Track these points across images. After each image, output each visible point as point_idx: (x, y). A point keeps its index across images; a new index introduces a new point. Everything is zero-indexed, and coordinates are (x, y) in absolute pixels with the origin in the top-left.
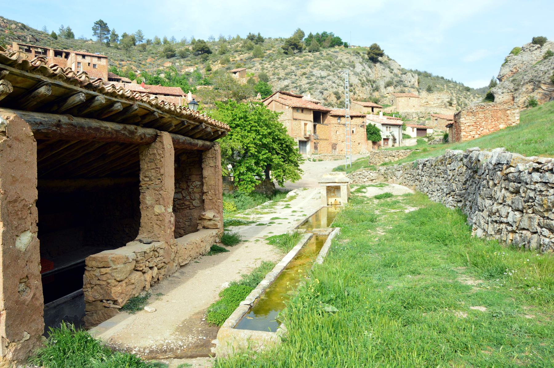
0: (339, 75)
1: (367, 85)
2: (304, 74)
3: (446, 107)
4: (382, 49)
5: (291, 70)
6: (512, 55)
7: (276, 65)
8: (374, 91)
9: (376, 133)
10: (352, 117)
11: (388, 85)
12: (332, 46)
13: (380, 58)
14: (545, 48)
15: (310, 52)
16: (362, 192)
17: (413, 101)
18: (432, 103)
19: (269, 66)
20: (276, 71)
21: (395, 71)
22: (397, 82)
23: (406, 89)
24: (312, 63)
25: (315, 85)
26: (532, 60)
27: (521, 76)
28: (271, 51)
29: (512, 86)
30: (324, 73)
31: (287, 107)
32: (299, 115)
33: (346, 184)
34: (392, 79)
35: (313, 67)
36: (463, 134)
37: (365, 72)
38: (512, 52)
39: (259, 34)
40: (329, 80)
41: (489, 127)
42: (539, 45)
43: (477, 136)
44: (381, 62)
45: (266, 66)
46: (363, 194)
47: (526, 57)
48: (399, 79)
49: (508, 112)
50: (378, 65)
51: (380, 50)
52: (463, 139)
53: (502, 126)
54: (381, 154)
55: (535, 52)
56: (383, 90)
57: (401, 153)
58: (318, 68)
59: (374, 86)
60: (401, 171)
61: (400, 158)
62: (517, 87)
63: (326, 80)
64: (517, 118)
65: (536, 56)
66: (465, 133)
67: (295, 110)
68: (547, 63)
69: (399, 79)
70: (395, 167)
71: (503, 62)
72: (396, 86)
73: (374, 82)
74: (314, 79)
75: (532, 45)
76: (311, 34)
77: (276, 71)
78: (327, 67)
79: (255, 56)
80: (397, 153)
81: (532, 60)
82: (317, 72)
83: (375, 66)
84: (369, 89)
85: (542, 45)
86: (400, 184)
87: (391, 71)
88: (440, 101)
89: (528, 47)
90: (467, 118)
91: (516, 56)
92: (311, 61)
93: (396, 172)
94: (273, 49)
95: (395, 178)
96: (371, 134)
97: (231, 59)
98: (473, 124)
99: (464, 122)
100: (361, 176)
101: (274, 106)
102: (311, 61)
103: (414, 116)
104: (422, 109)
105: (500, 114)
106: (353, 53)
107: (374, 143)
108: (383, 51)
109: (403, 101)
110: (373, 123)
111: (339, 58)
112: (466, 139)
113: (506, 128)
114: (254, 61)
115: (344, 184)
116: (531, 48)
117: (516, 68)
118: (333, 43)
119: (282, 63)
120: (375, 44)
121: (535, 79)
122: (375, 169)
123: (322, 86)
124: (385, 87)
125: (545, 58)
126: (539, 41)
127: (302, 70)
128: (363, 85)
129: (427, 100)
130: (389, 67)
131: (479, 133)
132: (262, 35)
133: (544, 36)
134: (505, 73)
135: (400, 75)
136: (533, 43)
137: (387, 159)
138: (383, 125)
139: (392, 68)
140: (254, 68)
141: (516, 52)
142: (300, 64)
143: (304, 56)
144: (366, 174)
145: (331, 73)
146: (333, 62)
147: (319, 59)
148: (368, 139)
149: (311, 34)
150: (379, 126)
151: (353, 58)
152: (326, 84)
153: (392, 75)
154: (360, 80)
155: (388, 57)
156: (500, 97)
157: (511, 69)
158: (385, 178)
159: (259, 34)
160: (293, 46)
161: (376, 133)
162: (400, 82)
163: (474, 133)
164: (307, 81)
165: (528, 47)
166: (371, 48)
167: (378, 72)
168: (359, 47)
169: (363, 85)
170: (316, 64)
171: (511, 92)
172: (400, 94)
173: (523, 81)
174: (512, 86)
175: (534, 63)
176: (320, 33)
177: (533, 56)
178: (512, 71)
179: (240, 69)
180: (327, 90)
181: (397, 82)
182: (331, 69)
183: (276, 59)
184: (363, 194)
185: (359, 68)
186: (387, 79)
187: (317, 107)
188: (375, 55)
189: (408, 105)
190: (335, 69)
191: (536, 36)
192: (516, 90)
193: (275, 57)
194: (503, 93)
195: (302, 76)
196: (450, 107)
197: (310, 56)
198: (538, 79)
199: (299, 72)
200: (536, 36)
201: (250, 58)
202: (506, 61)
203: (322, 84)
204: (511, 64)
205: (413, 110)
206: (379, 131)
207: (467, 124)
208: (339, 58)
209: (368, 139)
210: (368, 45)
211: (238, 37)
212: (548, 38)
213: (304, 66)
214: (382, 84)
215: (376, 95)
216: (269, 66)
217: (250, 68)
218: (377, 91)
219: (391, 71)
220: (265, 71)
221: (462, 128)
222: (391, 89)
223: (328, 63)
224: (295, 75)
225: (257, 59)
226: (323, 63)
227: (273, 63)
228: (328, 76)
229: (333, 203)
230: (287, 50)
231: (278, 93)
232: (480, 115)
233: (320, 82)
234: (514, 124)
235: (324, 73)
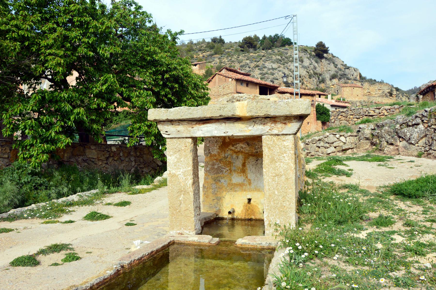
0: (289, 68)
1: (314, 77)
2: (258, 66)
3: (387, 96)
4: (327, 46)
5: (246, 63)
7: (233, 59)
8: (320, 82)
9: (325, 114)
10: (302, 95)
11: (333, 77)
12: (283, 45)
13: (325, 55)
15: (263, 50)
16: (340, 173)
17: (357, 91)
18: (374, 93)
19: (227, 60)
20: (233, 64)
21: (339, 66)
22: (341, 76)
23: (350, 81)
24: (265, 58)
25: (267, 75)
28: (230, 50)
30: (275, 66)
31: (230, 80)
32: (242, 88)
33: (293, 126)
34: (337, 72)
35: (265, 61)
37: (312, 66)
39: (220, 37)
40: (280, 71)
44: (326, 58)
45: (223, 60)
46: (346, 180)
48: (343, 72)
50: (323, 60)
51: (325, 47)
54: (350, 112)
56: (328, 82)
57: (384, 111)
58: (270, 62)
59: (321, 78)
60: (421, 126)
63: (276, 71)
67: (239, 84)
69: (343, 72)
70: (401, 121)
72: (340, 78)
73: (320, 75)
74: (266, 70)
76: (265, 36)
77: (233, 64)
78: (278, 61)
79: (216, 53)
80: (377, 111)
82: (268, 65)
83: (321, 61)
84: (315, 80)
86: (419, 156)
87: (336, 66)
88: (381, 92)
92: (263, 56)
93: (405, 130)
94: (232, 48)
95: (402, 144)
96: (320, 114)
97: (195, 56)
100: (322, 144)
101: (217, 80)
102: (263, 56)
103: (358, 104)
104: (366, 98)
106: (301, 50)
107: (324, 123)
108: (328, 48)
109: (348, 90)
110: (321, 104)
111: (289, 54)
114: (214, 57)
115: (278, 128)
118: (284, 43)
119: (238, 57)
120: (321, 42)
122: (349, 130)
123: (273, 76)
124: (331, 80)
127: (255, 63)
128: (310, 77)
129: (369, 91)
130: (334, 63)
132: (222, 38)
135: (343, 70)
138: (332, 106)
139: (336, 63)
140: (213, 63)
142: (254, 58)
143: (258, 52)
144: (332, 138)
145: (283, 66)
146: (283, 57)
147: (271, 54)
148: (318, 119)
149: (265, 36)
150: (328, 107)
151: (302, 54)
152: (276, 74)
153: (336, 69)
154: (308, 73)
155: (332, 55)
158: (373, 144)
159: (220, 37)
160: (249, 44)
161: (325, 114)
162: (344, 76)
164: (259, 72)
166: (317, 46)
167: (324, 67)
168: (307, 46)
169: (310, 77)
170: (269, 59)
172: (344, 85)
176: (273, 35)
179: (200, 62)
180: (277, 79)
181: (341, 76)
182: (281, 63)
183: (233, 55)
184: (346, 180)
185: (307, 62)
186: (332, 73)
187: (263, 82)
188: (320, 51)
189: (352, 94)
190: (285, 62)
193: (232, 53)
195: (255, 68)
196: (391, 97)
197: (263, 53)
199: (252, 65)
201: (211, 55)
203: (273, 74)
205: (357, 99)
206: (328, 111)
208: (289, 54)
209: (318, 119)
210: (313, 44)
211: (204, 40)
213: (258, 60)
214: (327, 76)
215: (322, 86)
216: (227, 60)
217: (210, 62)
218: (323, 83)
219: (336, 66)
220: (223, 64)
222: (335, 81)
223: (280, 58)
224: (249, 67)
225: (217, 55)
226: (274, 58)
227: (230, 58)
228: (279, 68)
229: (239, 213)
230: (243, 48)
231: (224, 70)
233: (271, 73)
235: (275, 66)
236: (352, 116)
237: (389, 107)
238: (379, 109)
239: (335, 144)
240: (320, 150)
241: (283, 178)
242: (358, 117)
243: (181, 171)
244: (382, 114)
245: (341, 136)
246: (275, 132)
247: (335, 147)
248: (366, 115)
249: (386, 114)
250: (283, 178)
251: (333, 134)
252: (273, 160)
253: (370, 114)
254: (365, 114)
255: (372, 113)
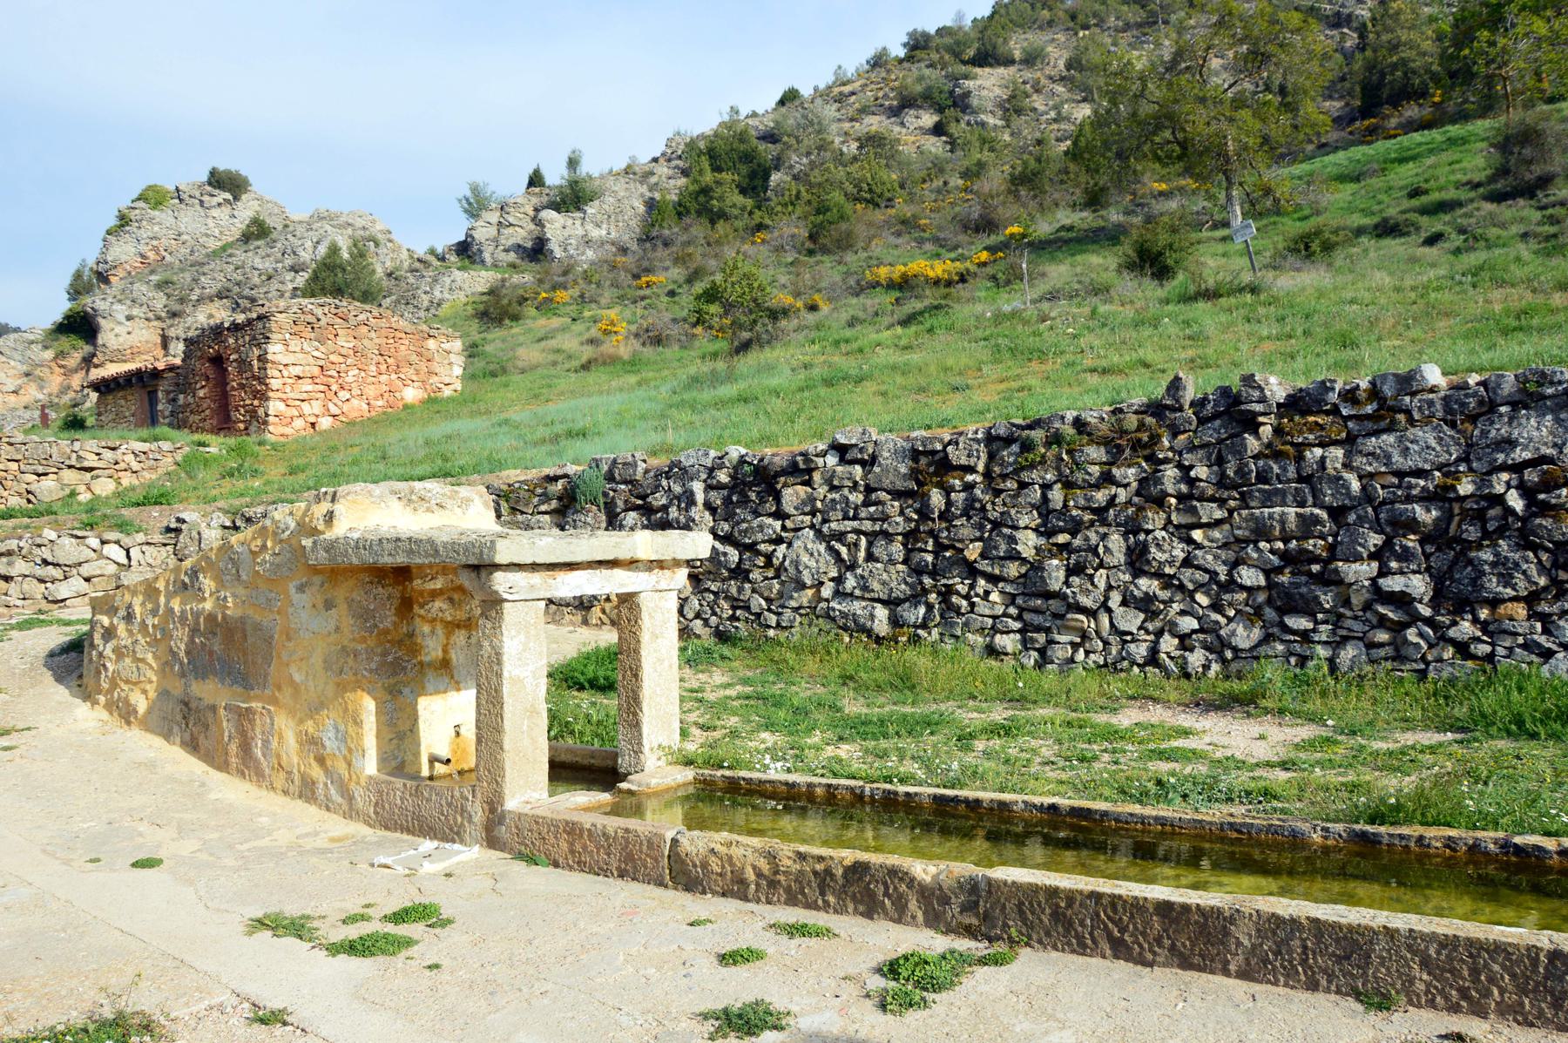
6: (141, 204)
14: (246, 210)
26: (207, 235)
27: (188, 276)
29: (160, 302)
36: (275, 406)
38: (141, 198)
41: (371, 391)
42: (228, 196)
43: (325, 423)
47: (189, 221)
49: (431, 343)
52: (275, 431)
53: (411, 394)
55: (215, 212)
57: (130, 458)
61: (127, 480)
62: (176, 307)
64: (458, 371)
65: (218, 225)
66: (281, 406)
68: (269, 251)
71: (112, 221)
75: (209, 188)
80: (108, 455)
81: (207, 235)
85: (236, 198)
89: (197, 194)
90: (295, 344)
91: (157, 213)
98: (316, 371)
99: (277, 358)
100: (20, 567)
105: (404, 349)
112: (288, 430)
113: (422, 402)
116: (206, 198)
117: (156, 249)
121: (236, 289)
125: (246, 238)
126: (227, 183)
131: (334, 410)
133: (243, 173)
134: (124, 258)
136: (210, 184)
137: (48, 483)
141: (153, 197)
156: (118, 329)
157: (143, 248)
163: (316, 407)
165: (197, 194)
171: (159, 318)
173: (197, 291)
174: (160, 302)
175: (213, 244)
177: (210, 222)
178: (142, 256)
191: (222, 166)
192: (174, 315)
194: (129, 318)
198: (246, 292)
200: (222, 167)
202: (124, 220)
204: (143, 234)
207: (297, 371)
212: (251, 180)
221: (274, 383)
232: (341, 341)
234: (447, 392)
236: (14, 466)
237: (145, 446)
238: (113, 449)
239: (86, 570)
240: (13, 588)
241: (666, 663)
242: (41, 469)
243: (531, 667)
244: (122, 466)
245: (103, 542)
246: (663, 586)
247: (87, 580)
248: (70, 467)
249: (135, 466)
250: (666, 663)
251: (77, 537)
252: (655, 636)
253: (86, 464)
254: (68, 462)
255: (91, 461)
